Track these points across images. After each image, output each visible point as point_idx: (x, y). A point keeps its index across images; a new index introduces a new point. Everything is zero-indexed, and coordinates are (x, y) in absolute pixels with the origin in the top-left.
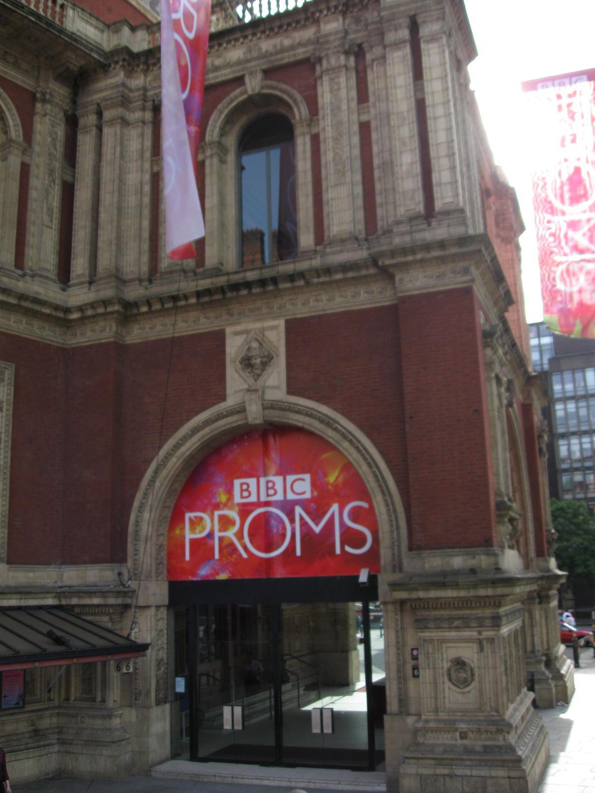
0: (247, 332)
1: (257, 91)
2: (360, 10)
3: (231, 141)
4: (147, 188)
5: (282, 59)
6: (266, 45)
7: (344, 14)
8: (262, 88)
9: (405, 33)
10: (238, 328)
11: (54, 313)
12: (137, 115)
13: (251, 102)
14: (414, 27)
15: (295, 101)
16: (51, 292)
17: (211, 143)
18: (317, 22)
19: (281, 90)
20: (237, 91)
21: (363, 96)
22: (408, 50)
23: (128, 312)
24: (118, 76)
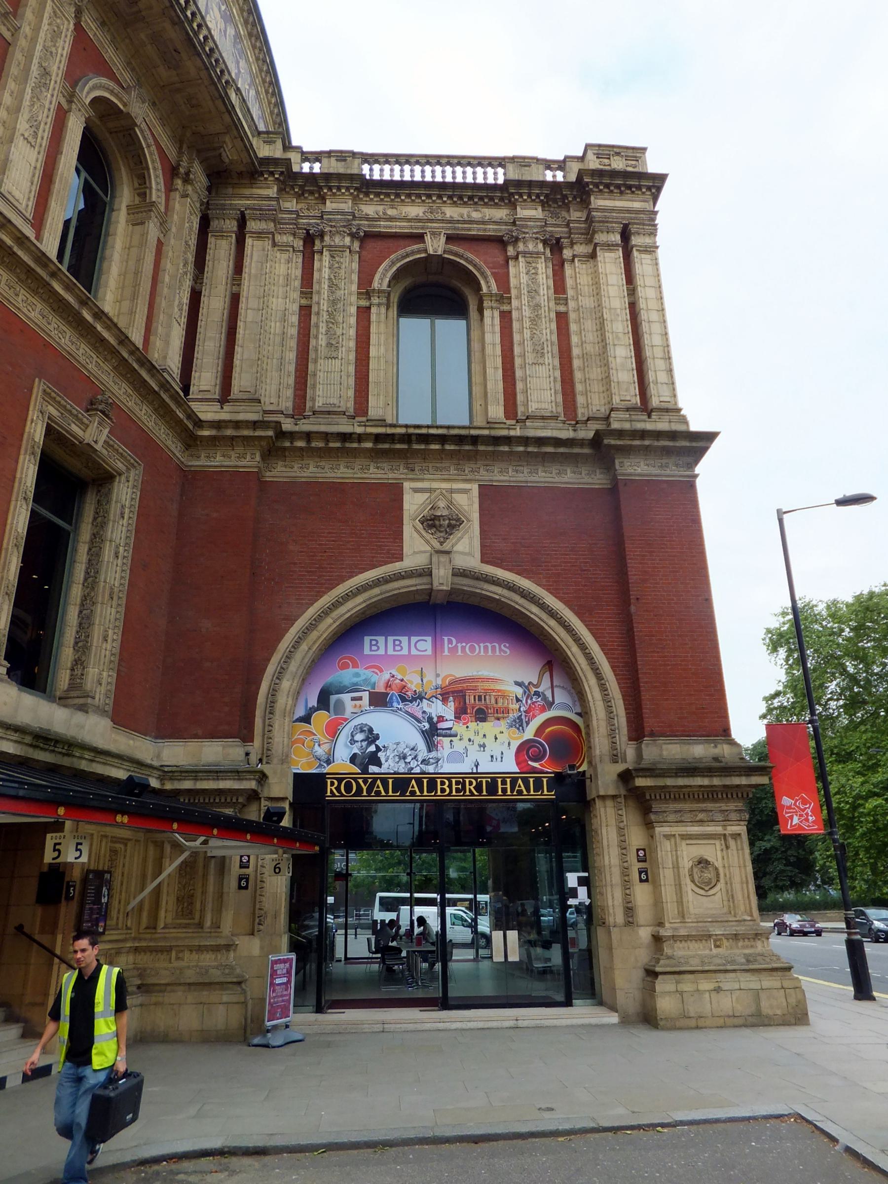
0: (430, 490)
1: (439, 253)
2: (559, 207)
5: (469, 230)
6: (451, 212)
7: (543, 204)
8: (445, 252)
10: (419, 485)
13: (429, 263)
14: (626, 235)
15: (483, 274)
17: (379, 291)
18: (513, 206)
19: (466, 260)
20: (415, 247)
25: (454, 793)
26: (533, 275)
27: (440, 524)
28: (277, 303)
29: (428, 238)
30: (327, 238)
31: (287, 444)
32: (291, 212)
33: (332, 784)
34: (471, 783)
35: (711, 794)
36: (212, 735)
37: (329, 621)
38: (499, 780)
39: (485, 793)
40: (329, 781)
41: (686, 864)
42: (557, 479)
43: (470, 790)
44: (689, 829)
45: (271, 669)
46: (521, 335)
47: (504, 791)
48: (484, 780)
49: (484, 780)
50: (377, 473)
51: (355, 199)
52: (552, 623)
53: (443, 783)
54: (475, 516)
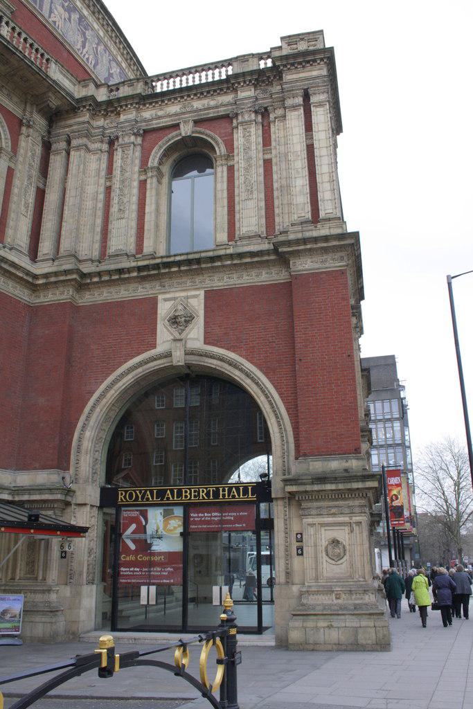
0: (175, 299)
1: (189, 134)
2: (267, 85)
3: (166, 169)
4: (101, 197)
5: (208, 114)
6: (197, 104)
7: (255, 86)
8: (193, 132)
9: (300, 100)
10: (168, 296)
11: (25, 277)
12: (98, 145)
14: (306, 96)
15: (216, 142)
16: (25, 262)
17: (152, 168)
18: (235, 90)
19: (206, 135)
20: (174, 133)
21: (267, 141)
22: (302, 111)
23: (83, 282)
24: (86, 117)
25: (193, 498)
26: (247, 137)
27: (179, 321)
28: (90, 189)
29: (181, 126)
30: (120, 140)
31: (89, 281)
32: (99, 128)
33: (122, 494)
34: (203, 491)
35: (340, 495)
36: (44, 467)
37: (112, 392)
38: (221, 489)
39: (211, 497)
40: (120, 492)
41: (324, 543)
42: (256, 280)
43: (203, 496)
44: (326, 519)
45: (80, 424)
46: (240, 180)
47: (224, 495)
48: (211, 489)
49: (211, 489)
50: (141, 291)
51: (138, 109)
52: (249, 381)
53: (186, 492)
54: (202, 313)
